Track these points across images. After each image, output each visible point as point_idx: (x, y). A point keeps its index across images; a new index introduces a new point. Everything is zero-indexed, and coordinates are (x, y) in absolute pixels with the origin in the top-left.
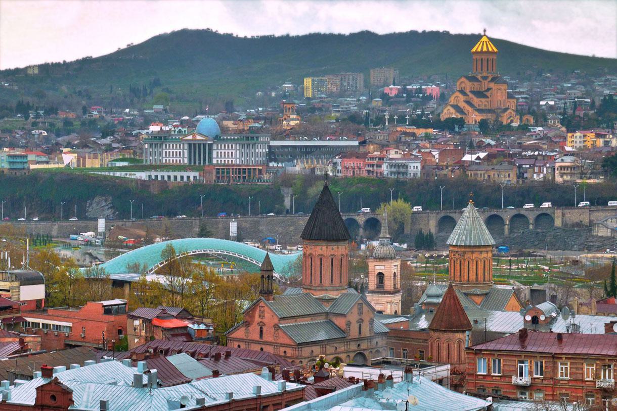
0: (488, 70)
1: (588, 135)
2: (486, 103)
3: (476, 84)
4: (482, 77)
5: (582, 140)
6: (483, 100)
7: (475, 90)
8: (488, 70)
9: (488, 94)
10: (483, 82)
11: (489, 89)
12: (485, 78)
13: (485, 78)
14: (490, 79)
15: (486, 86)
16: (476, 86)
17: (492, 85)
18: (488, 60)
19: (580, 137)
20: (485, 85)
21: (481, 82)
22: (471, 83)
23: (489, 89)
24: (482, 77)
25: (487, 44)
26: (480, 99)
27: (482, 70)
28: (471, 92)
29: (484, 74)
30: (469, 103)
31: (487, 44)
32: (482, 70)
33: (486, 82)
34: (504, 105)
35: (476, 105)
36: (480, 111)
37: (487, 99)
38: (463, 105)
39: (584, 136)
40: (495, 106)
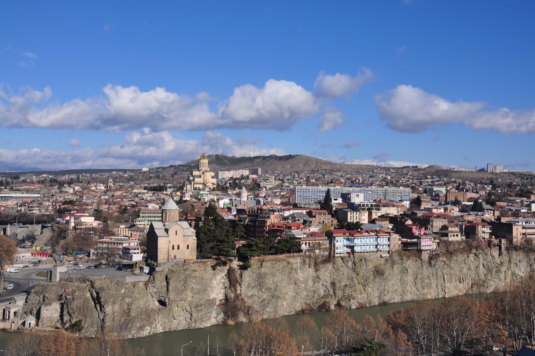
7: (197, 175)
34: (208, 181)
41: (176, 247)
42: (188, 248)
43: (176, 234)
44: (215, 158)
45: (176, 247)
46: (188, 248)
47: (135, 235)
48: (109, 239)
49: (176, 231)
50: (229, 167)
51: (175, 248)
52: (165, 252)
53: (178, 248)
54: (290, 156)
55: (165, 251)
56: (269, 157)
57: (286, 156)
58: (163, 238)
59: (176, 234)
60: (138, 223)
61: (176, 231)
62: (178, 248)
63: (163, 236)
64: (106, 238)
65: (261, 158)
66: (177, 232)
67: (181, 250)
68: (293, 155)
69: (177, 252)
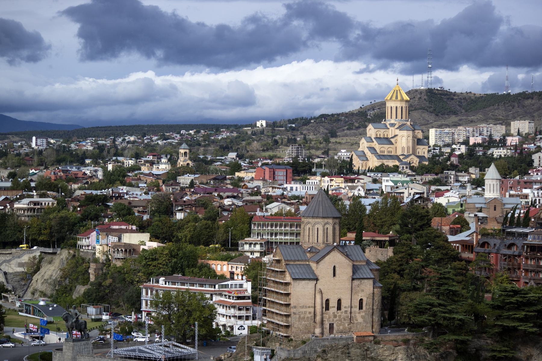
0: (396, 118)
1: (334, 179)
3: (382, 131)
4: (389, 124)
6: (387, 146)
7: (382, 136)
8: (396, 118)
9: (393, 140)
10: (391, 128)
11: (396, 136)
12: (392, 125)
13: (392, 125)
14: (396, 127)
15: (393, 133)
16: (381, 133)
17: (397, 132)
18: (397, 107)
20: (391, 132)
21: (389, 129)
22: (376, 130)
23: (396, 136)
24: (389, 124)
25: (397, 93)
26: (382, 146)
27: (391, 118)
28: (376, 138)
29: (393, 121)
30: (372, 150)
31: (397, 93)
32: (391, 118)
33: (393, 128)
35: (378, 151)
36: (380, 157)
37: (391, 146)
38: (367, 151)
39: (331, 180)
40: (399, 152)
41: (333, 303)
42: (361, 307)
43: (334, 275)
44: (426, 97)
45: (333, 303)
49: (334, 267)
50: (459, 118)
51: (331, 305)
52: (309, 316)
53: (339, 308)
55: (310, 313)
58: (304, 282)
59: (334, 275)
60: (247, 247)
61: (334, 267)
62: (339, 308)
63: (304, 279)
65: (536, 97)
69: (335, 316)
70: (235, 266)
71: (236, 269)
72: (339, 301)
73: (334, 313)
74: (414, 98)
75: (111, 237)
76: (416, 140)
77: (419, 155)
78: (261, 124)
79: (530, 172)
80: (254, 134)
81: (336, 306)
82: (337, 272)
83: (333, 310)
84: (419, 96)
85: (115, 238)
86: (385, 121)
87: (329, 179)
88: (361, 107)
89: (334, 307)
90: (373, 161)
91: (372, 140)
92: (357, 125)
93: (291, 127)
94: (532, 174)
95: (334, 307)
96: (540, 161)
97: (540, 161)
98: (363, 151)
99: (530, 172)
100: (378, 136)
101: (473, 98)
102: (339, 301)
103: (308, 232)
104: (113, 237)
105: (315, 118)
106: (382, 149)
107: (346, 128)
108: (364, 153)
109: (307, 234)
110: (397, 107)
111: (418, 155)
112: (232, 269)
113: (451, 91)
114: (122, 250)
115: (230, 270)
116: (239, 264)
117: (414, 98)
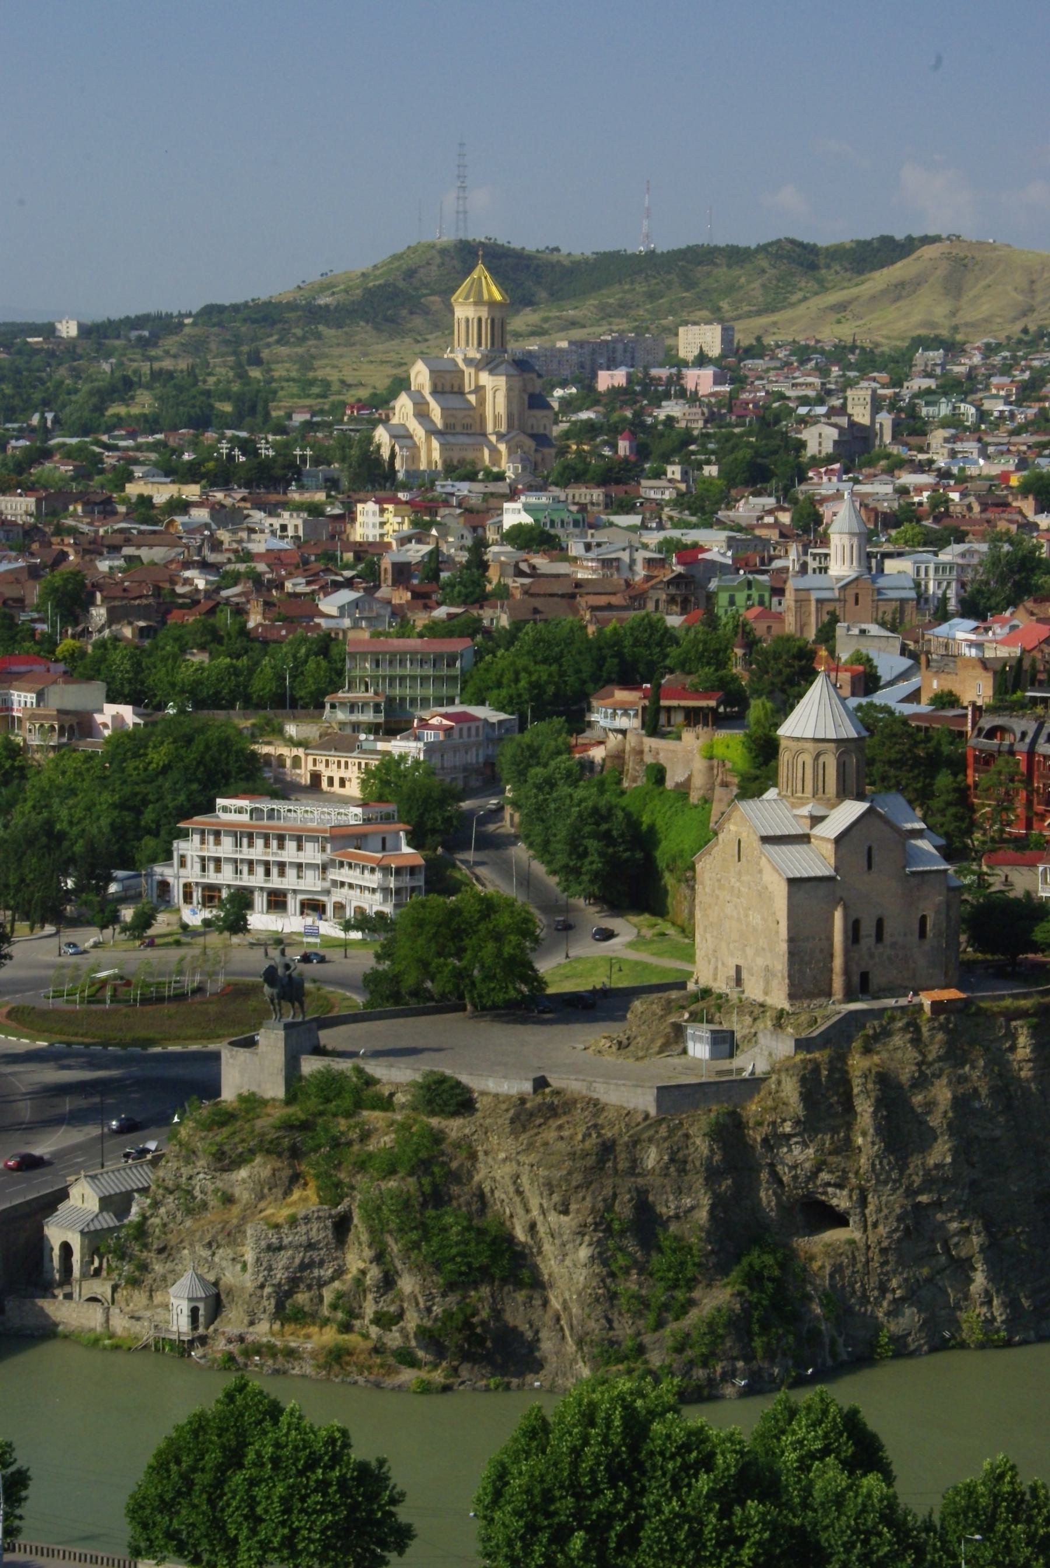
2: (468, 421)
5: (378, 520)
8: (480, 344)
19: (374, 513)
27: (467, 344)
41: (868, 928)
42: (922, 934)
43: (870, 867)
44: (455, 262)
45: (868, 928)
46: (922, 934)
47: (336, 782)
48: (240, 811)
49: (870, 849)
53: (879, 937)
54: (887, 241)
56: (762, 249)
57: (864, 246)
58: (808, 885)
59: (870, 867)
61: (870, 849)
62: (879, 937)
64: (225, 809)
66: (874, 852)
67: (894, 945)
68: (900, 236)
70: (343, 760)
71: (327, 765)
72: (880, 923)
73: (869, 949)
74: (429, 264)
75: (16, 693)
76: (526, 397)
77: (535, 431)
78: (69, 329)
79: (811, 474)
80: (52, 354)
81: (873, 933)
82: (876, 859)
83: (868, 941)
84: (438, 260)
85: (29, 695)
86: (452, 352)
87: (376, 507)
88: (299, 287)
89: (869, 936)
90: (429, 451)
91: (423, 397)
92: (298, 332)
93: (140, 338)
94: (816, 480)
95: (869, 936)
96: (820, 444)
97: (820, 444)
98: (404, 425)
99: (811, 474)
100: (439, 389)
101: (566, 263)
102: (880, 923)
103: (800, 771)
104: (23, 694)
105: (189, 315)
106: (452, 421)
107: (271, 340)
108: (407, 430)
109: (800, 775)
110: (480, 320)
111: (530, 431)
112: (315, 764)
113: (512, 246)
114: (52, 727)
115: (310, 766)
116: (332, 753)
117: (429, 264)
